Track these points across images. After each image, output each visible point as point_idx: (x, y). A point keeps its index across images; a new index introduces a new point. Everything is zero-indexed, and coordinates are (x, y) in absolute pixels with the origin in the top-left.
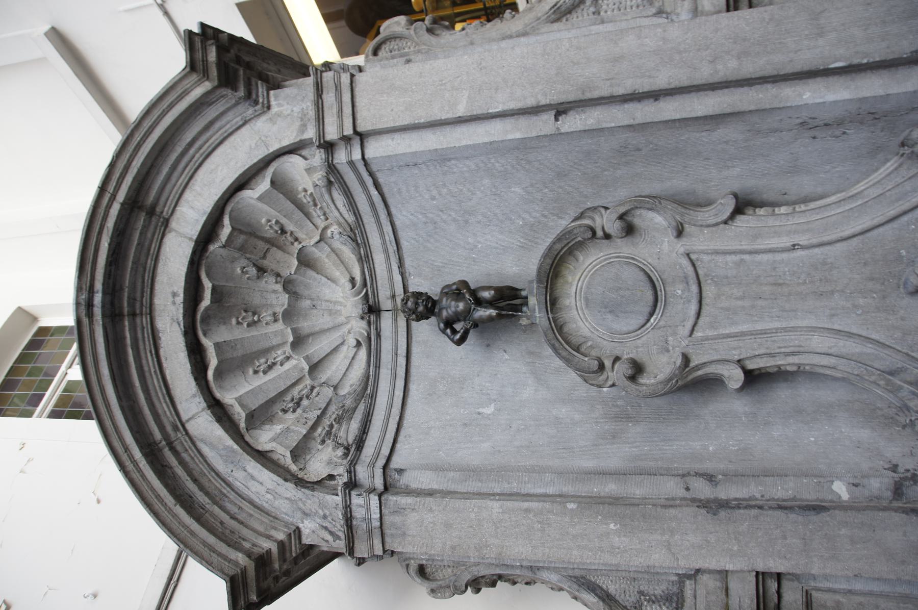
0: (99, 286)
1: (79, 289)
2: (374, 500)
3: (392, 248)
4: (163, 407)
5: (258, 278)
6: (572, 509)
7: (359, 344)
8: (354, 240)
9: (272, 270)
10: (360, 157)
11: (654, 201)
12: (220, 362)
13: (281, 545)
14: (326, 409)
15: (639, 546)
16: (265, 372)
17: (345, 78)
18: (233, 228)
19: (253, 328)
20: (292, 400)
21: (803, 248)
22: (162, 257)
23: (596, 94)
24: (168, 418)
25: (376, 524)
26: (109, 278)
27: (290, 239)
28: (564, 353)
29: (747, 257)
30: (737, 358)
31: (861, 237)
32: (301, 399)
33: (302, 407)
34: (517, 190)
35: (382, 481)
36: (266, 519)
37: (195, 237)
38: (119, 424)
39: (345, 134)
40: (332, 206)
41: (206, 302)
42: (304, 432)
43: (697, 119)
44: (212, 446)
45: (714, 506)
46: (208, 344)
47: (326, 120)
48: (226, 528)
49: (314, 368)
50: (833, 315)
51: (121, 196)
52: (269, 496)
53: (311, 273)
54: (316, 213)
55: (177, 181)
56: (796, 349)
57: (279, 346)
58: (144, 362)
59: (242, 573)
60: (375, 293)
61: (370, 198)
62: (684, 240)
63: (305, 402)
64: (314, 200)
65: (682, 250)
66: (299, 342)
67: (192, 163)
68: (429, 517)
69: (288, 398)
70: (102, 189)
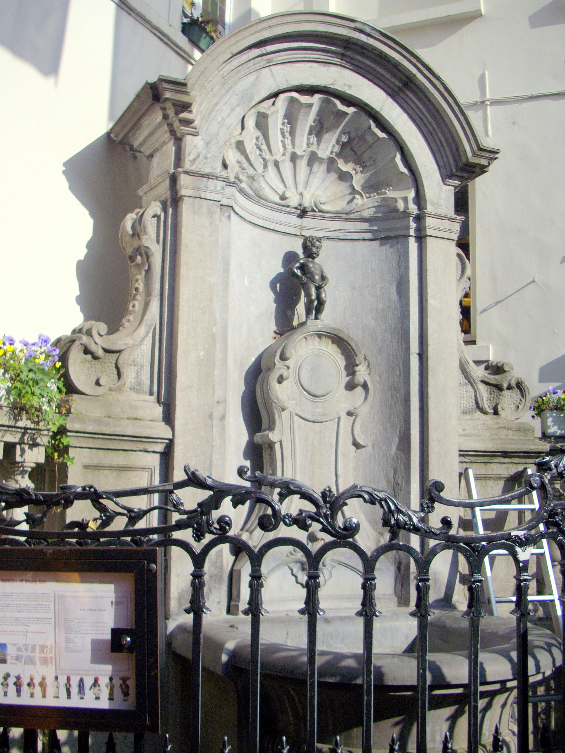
0: (371, 41)
12: (301, 104)
16: (282, 130)
18: (379, 138)
21: (337, 481)
30: (283, 439)
32: (260, 150)
37: (381, 113)
41: (341, 107)
42: (248, 151)
45: (211, 417)
49: (276, 164)
52: (220, 119)
66: (294, 158)
69: (264, 142)
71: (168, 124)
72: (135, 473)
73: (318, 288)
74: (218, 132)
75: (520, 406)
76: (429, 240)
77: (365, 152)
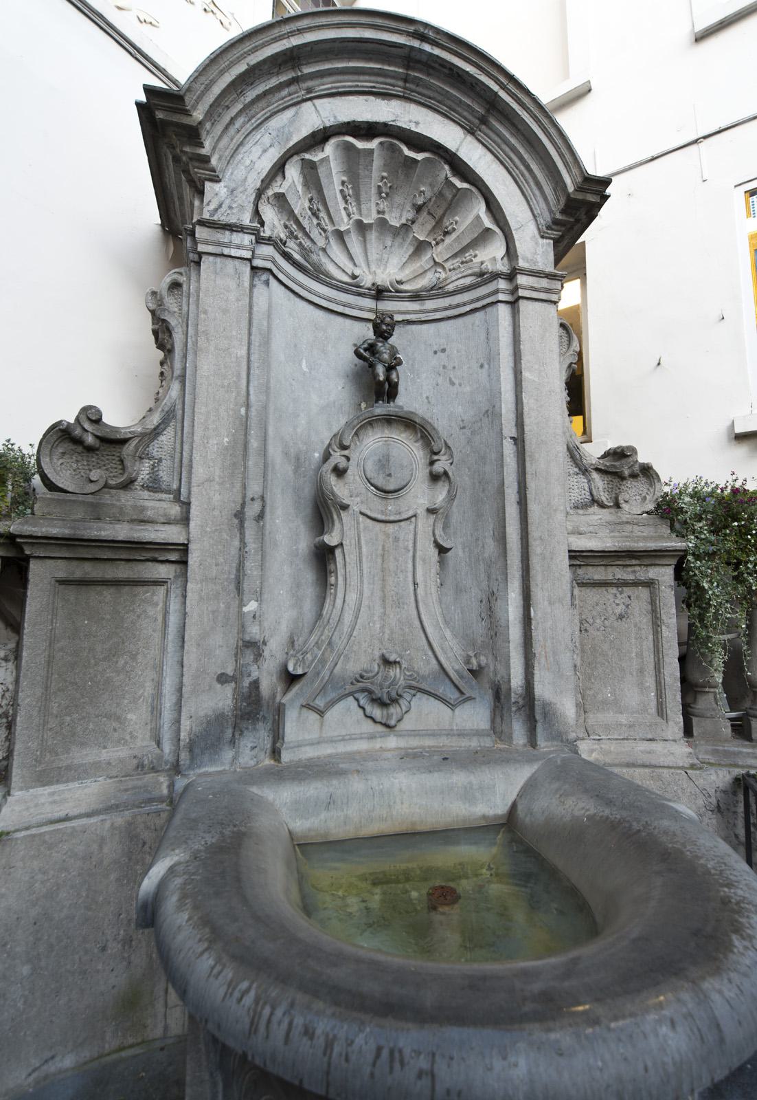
0: (437, 51)
1: (437, 31)
2: (248, 254)
3: (423, 317)
4: (327, 85)
5: (414, 205)
6: (240, 411)
7: (354, 277)
8: (432, 289)
9: (417, 218)
11: (451, 497)
12: (358, 151)
13: (205, 160)
14: (309, 237)
15: (209, 458)
16: (342, 191)
17: (554, 297)
18: (459, 189)
19: (376, 191)
20: (318, 210)
22: (447, 121)
23: (528, 464)
24: (319, 85)
25: (226, 251)
26: (441, 65)
27: (439, 238)
28: (355, 422)
29: (411, 554)
30: (344, 543)
31: (419, 626)
32: (318, 218)
33: (312, 217)
34: (460, 409)
35: (260, 266)
36: (228, 153)
38: (321, 32)
39: (520, 290)
40: (460, 275)
41: (407, 152)
42: (296, 212)
43: (505, 527)
44: (292, 121)
45: (240, 515)
46: (374, 144)
47: (530, 277)
48: (223, 110)
49: (340, 236)
50: (369, 607)
51: (502, 94)
52: (248, 162)
53: (411, 250)
54: (456, 262)
55: (501, 150)
56: (348, 582)
57: (360, 210)
58: (367, 78)
59: (187, 111)
60: (391, 298)
61: (464, 304)
62: (425, 513)
63: (315, 221)
64: (466, 262)
65: (419, 512)
67: (512, 166)
68: (232, 297)
69: (321, 207)
70: (512, 78)
71: (184, 171)
72: (145, 588)
74: (246, 177)
75: (647, 496)
77: (444, 215)
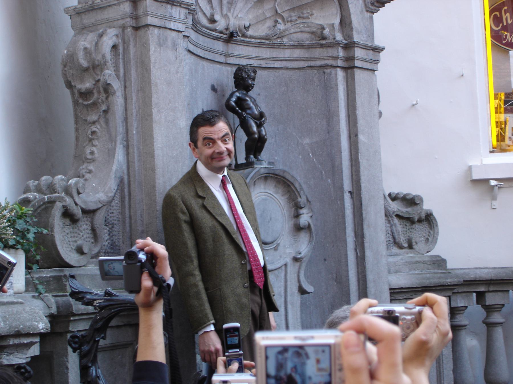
10: (339, 65)
40: (299, 30)
47: (363, 50)
54: (294, 15)
64: (303, 18)
73: (259, 126)
76: (357, 72)
